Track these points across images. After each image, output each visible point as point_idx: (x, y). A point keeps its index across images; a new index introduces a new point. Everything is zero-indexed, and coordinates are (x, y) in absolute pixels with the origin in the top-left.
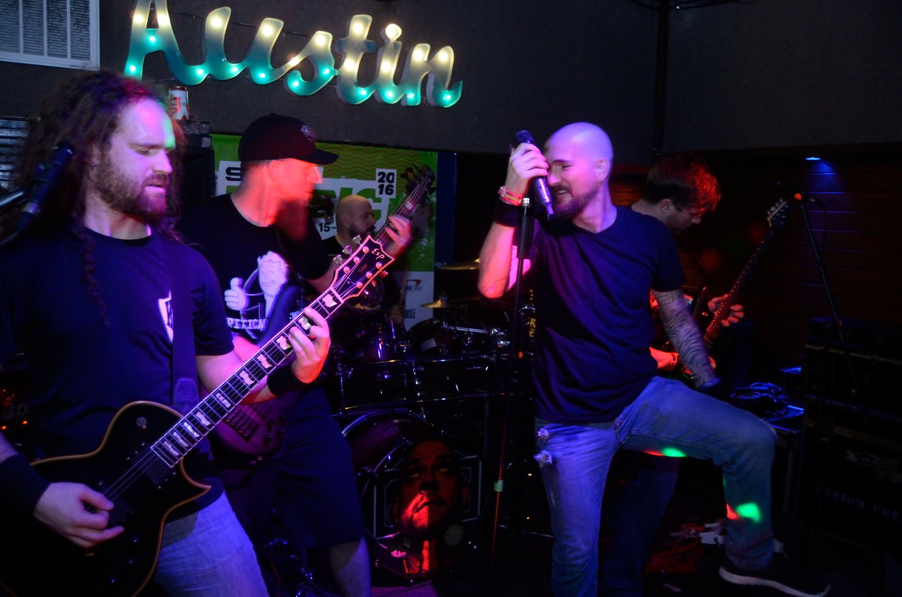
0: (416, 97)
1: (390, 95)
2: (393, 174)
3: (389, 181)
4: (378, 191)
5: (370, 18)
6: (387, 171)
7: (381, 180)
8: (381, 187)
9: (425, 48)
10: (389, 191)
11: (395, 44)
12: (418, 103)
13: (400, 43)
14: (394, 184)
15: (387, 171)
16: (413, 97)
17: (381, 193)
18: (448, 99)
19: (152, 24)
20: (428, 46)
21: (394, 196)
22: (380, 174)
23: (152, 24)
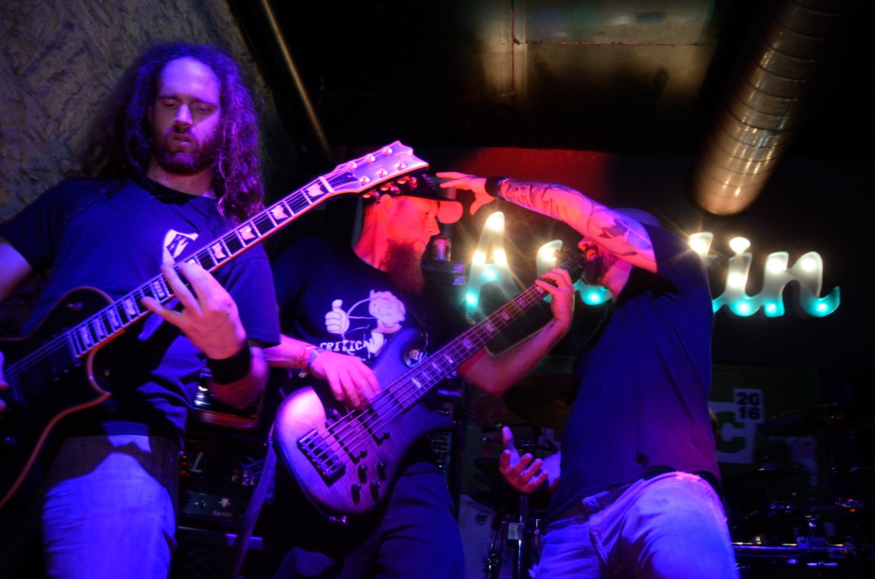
0: (778, 308)
1: (744, 308)
2: (756, 395)
3: (752, 403)
4: (738, 414)
5: (710, 235)
6: (749, 391)
7: (741, 402)
8: (742, 410)
9: (782, 257)
10: (754, 414)
11: (745, 259)
12: (782, 311)
13: (750, 255)
14: (760, 406)
15: (749, 391)
16: (774, 309)
17: (743, 417)
18: (822, 307)
19: (489, 261)
20: (785, 254)
21: (760, 421)
22: (740, 394)
23: (489, 261)
